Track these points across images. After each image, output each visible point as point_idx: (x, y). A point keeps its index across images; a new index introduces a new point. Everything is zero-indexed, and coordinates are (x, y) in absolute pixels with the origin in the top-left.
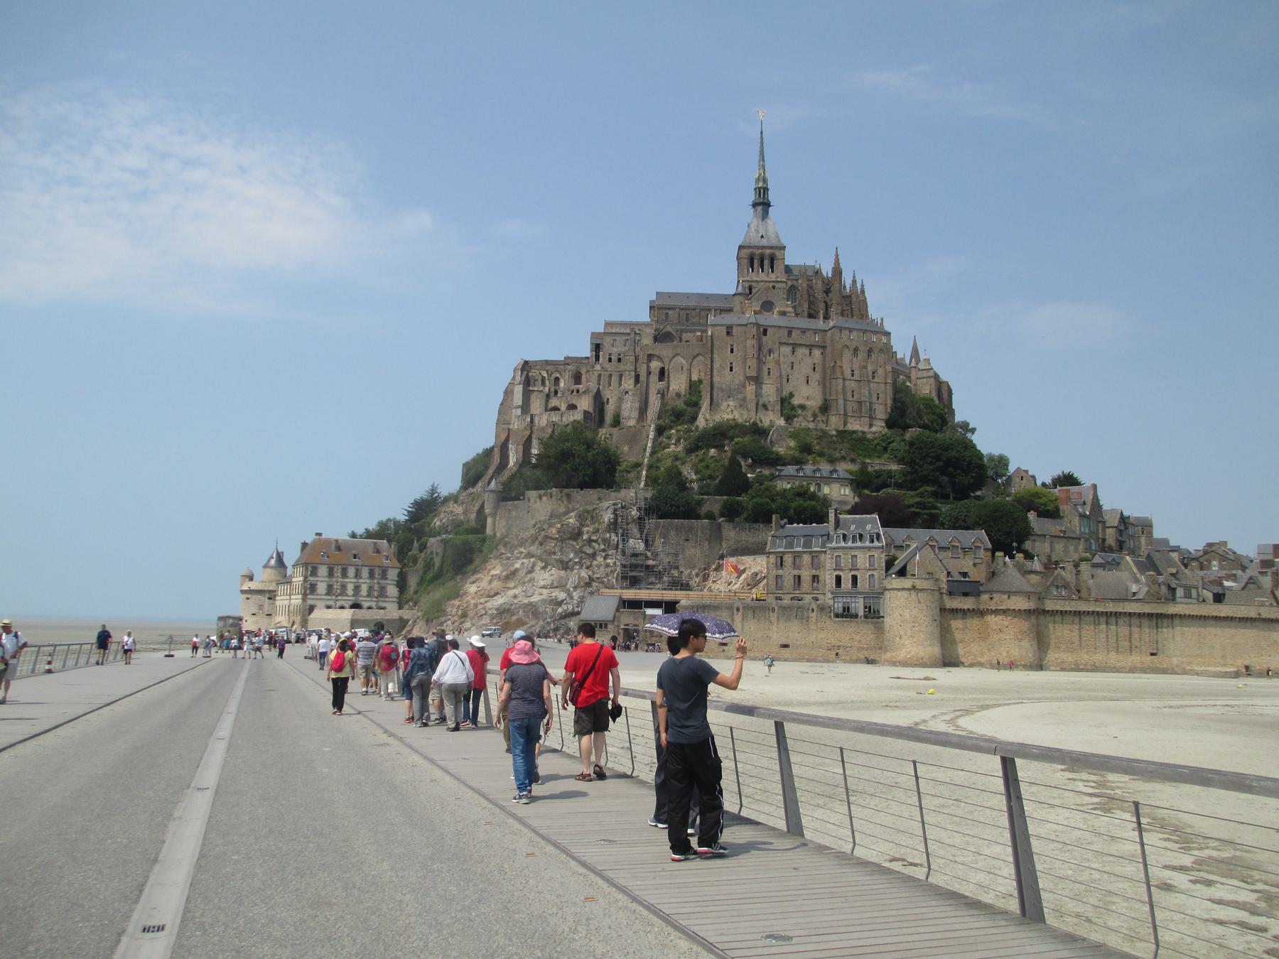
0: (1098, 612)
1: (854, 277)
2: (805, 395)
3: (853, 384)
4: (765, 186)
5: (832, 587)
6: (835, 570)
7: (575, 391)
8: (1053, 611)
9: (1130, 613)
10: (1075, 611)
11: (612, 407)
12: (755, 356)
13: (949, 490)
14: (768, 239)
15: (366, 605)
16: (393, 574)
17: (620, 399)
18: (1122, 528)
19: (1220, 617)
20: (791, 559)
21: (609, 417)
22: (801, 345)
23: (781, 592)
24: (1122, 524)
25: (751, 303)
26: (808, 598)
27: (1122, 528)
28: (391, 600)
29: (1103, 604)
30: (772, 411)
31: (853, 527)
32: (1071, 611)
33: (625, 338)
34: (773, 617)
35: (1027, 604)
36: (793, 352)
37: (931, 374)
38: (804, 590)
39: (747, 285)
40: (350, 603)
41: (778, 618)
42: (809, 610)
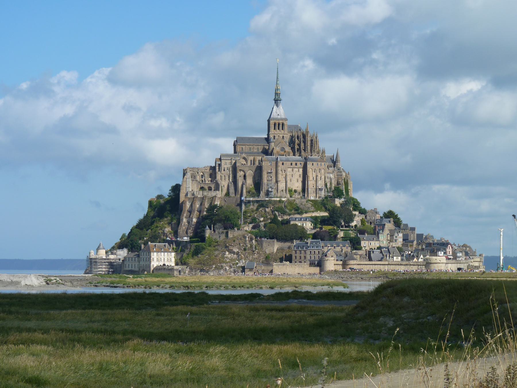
2: (297, 186)
3: (313, 183)
4: (279, 92)
7: (210, 181)
13: (343, 224)
14: (281, 116)
15: (166, 264)
16: (173, 254)
18: (397, 235)
24: (397, 234)
27: (397, 235)
28: (173, 262)
33: (230, 161)
34: (296, 267)
36: (293, 170)
37: (341, 174)
39: (273, 135)
40: (163, 264)
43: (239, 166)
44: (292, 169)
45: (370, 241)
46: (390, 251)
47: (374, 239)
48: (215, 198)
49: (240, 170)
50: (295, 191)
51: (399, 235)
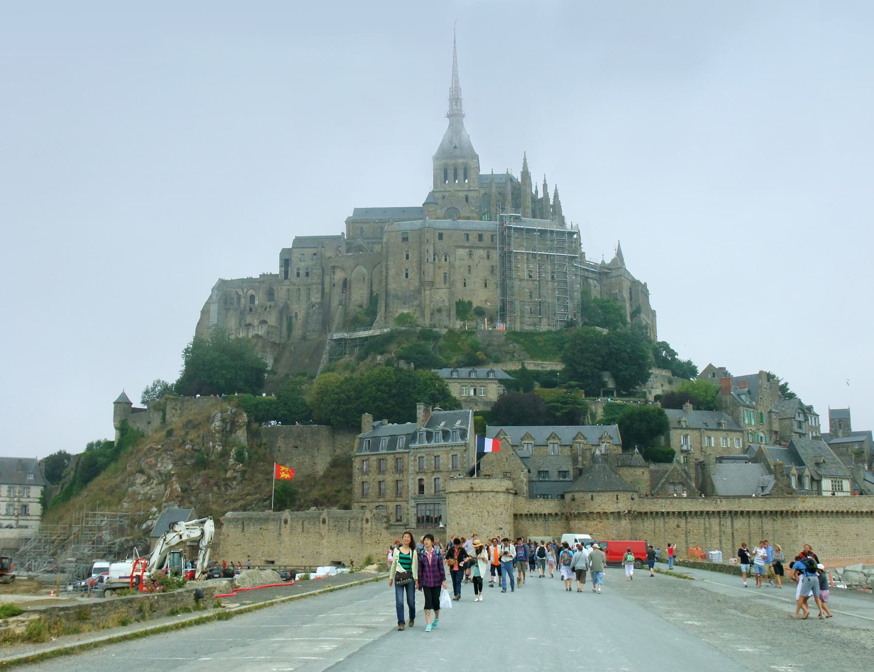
0: (708, 512)
1: (545, 181)
2: (483, 299)
5: (415, 493)
6: (417, 473)
7: (268, 307)
8: (652, 513)
9: (748, 512)
10: (679, 513)
11: (300, 322)
12: (429, 260)
13: (611, 385)
16: (36, 492)
17: (307, 314)
18: (801, 418)
19: (862, 512)
20: (375, 463)
21: (297, 333)
22: (478, 248)
23: (366, 500)
24: (801, 415)
25: (435, 210)
26: (392, 506)
27: (801, 418)
28: (33, 518)
29: (714, 502)
30: (449, 316)
31: (443, 424)
32: (674, 513)
34: (324, 529)
35: (615, 505)
36: (470, 255)
37: (619, 273)
38: (388, 497)
41: (329, 530)
42: (362, 520)
43: (330, 258)
44: (467, 250)
45: (706, 429)
46: (801, 452)
47: (720, 424)
48: (255, 341)
49: (334, 268)
50: (480, 312)
51: (810, 419)
